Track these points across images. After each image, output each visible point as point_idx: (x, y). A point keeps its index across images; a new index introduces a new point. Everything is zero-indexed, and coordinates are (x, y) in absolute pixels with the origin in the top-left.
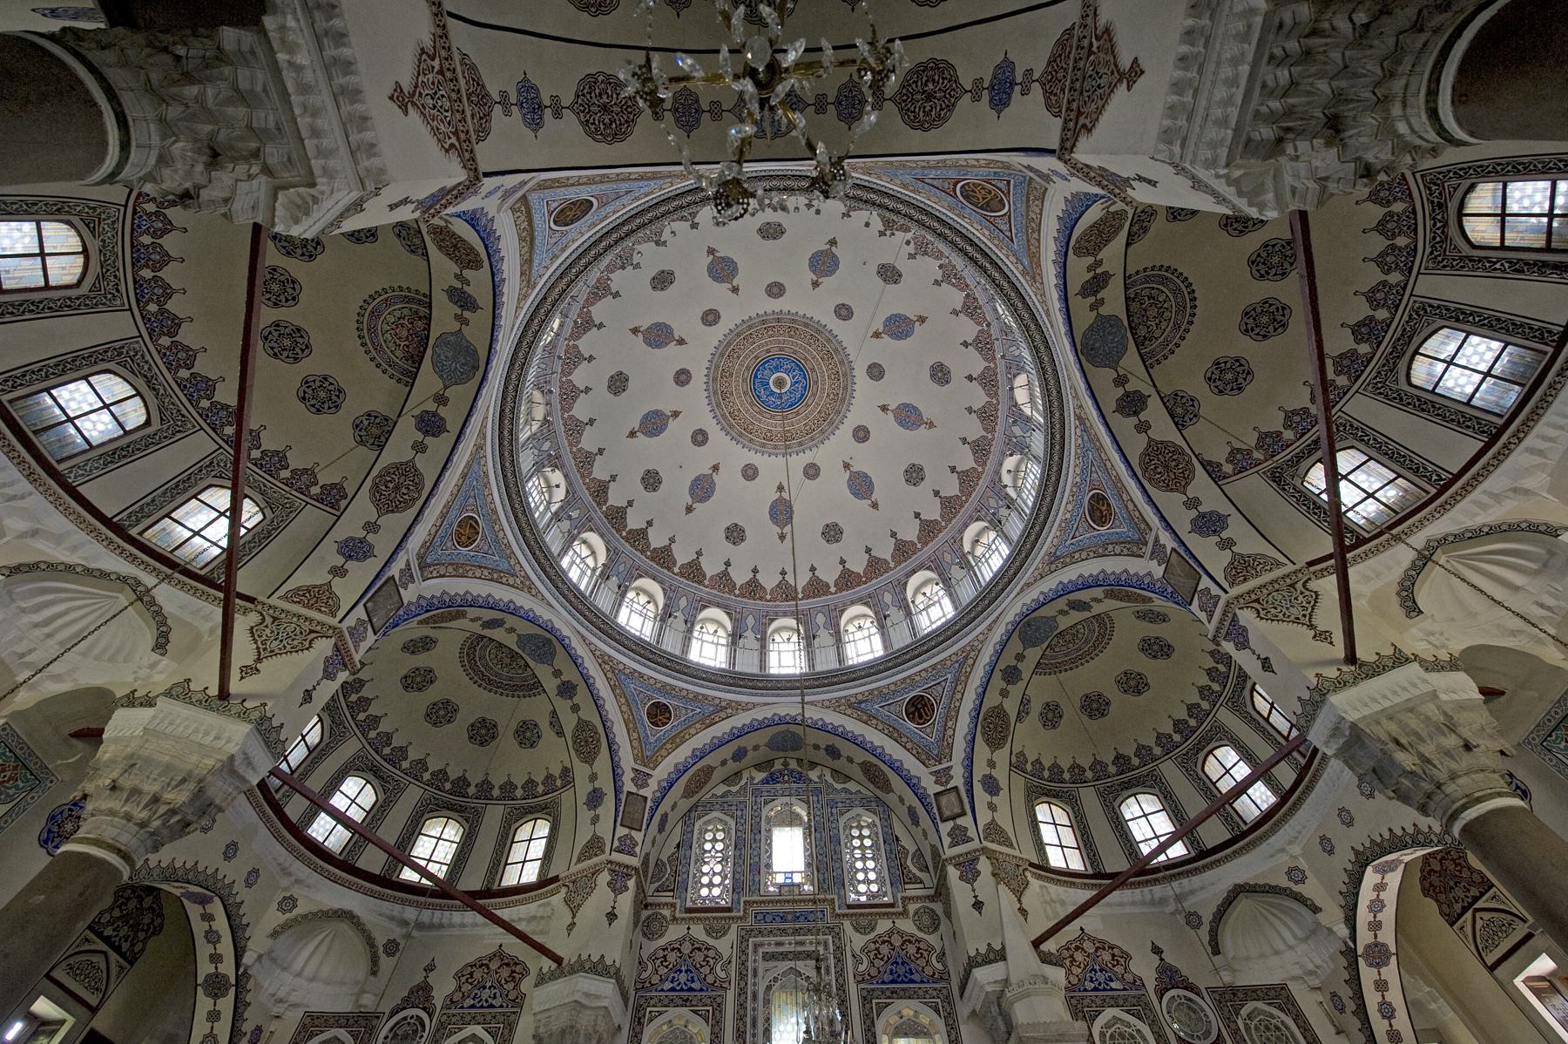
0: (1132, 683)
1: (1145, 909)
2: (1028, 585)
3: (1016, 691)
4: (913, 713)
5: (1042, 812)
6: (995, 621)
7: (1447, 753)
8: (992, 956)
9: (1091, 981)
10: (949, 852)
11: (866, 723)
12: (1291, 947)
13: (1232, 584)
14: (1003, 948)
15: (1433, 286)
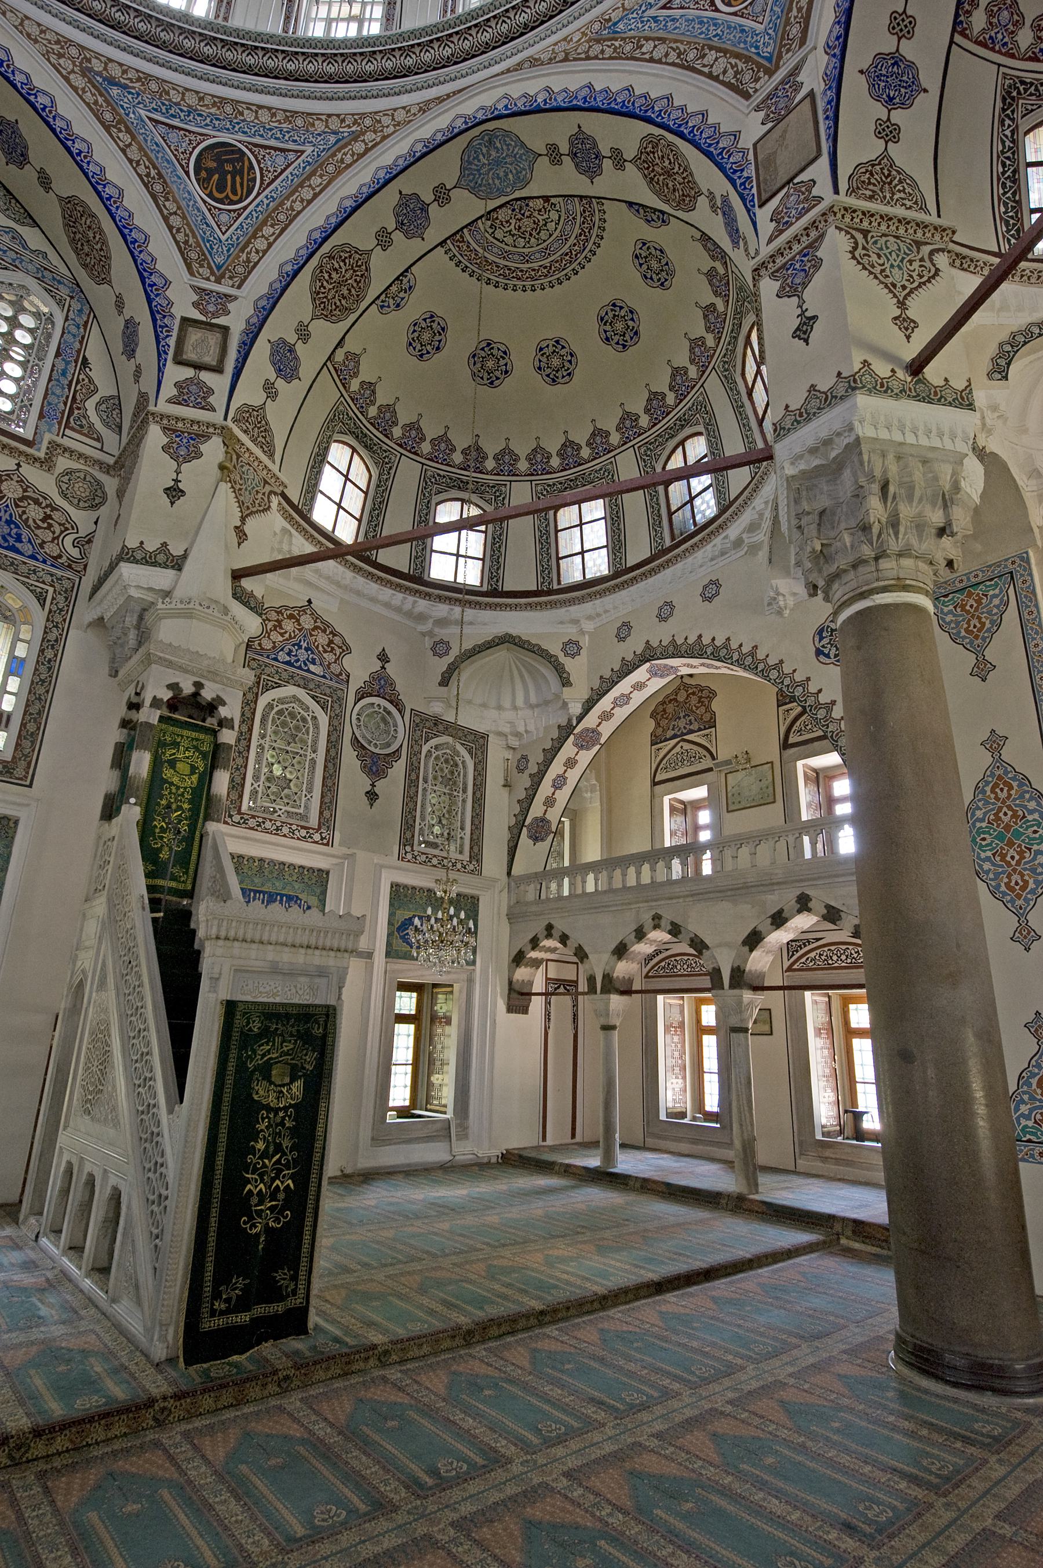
0: (556, 362)
1: (397, 617)
2: (534, 62)
3: (405, 248)
4: (210, 172)
5: (338, 454)
6: (440, 100)
7: (920, 527)
8: (161, 558)
9: (289, 654)
10: (163, 407)
11: (107, 128)
12: (515, 708)
13: (851, 191)
14: (185, 556)
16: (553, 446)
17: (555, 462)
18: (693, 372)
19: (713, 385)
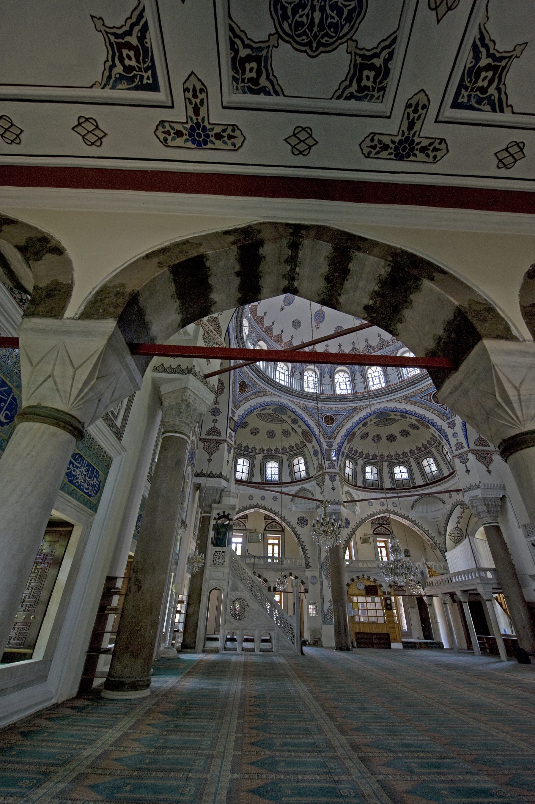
2: (294, 403)
6: (278, 396)
15: (385, 465)
16: (244, 445)
17: (243, 448)
18: (281, 451)
19: (285, 457)
